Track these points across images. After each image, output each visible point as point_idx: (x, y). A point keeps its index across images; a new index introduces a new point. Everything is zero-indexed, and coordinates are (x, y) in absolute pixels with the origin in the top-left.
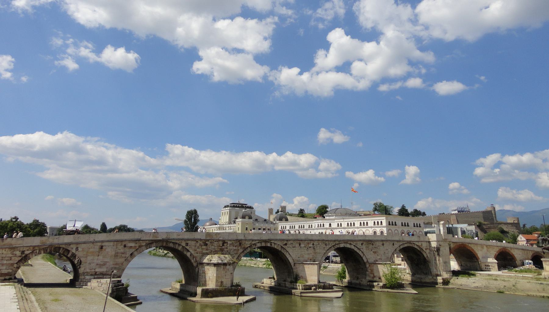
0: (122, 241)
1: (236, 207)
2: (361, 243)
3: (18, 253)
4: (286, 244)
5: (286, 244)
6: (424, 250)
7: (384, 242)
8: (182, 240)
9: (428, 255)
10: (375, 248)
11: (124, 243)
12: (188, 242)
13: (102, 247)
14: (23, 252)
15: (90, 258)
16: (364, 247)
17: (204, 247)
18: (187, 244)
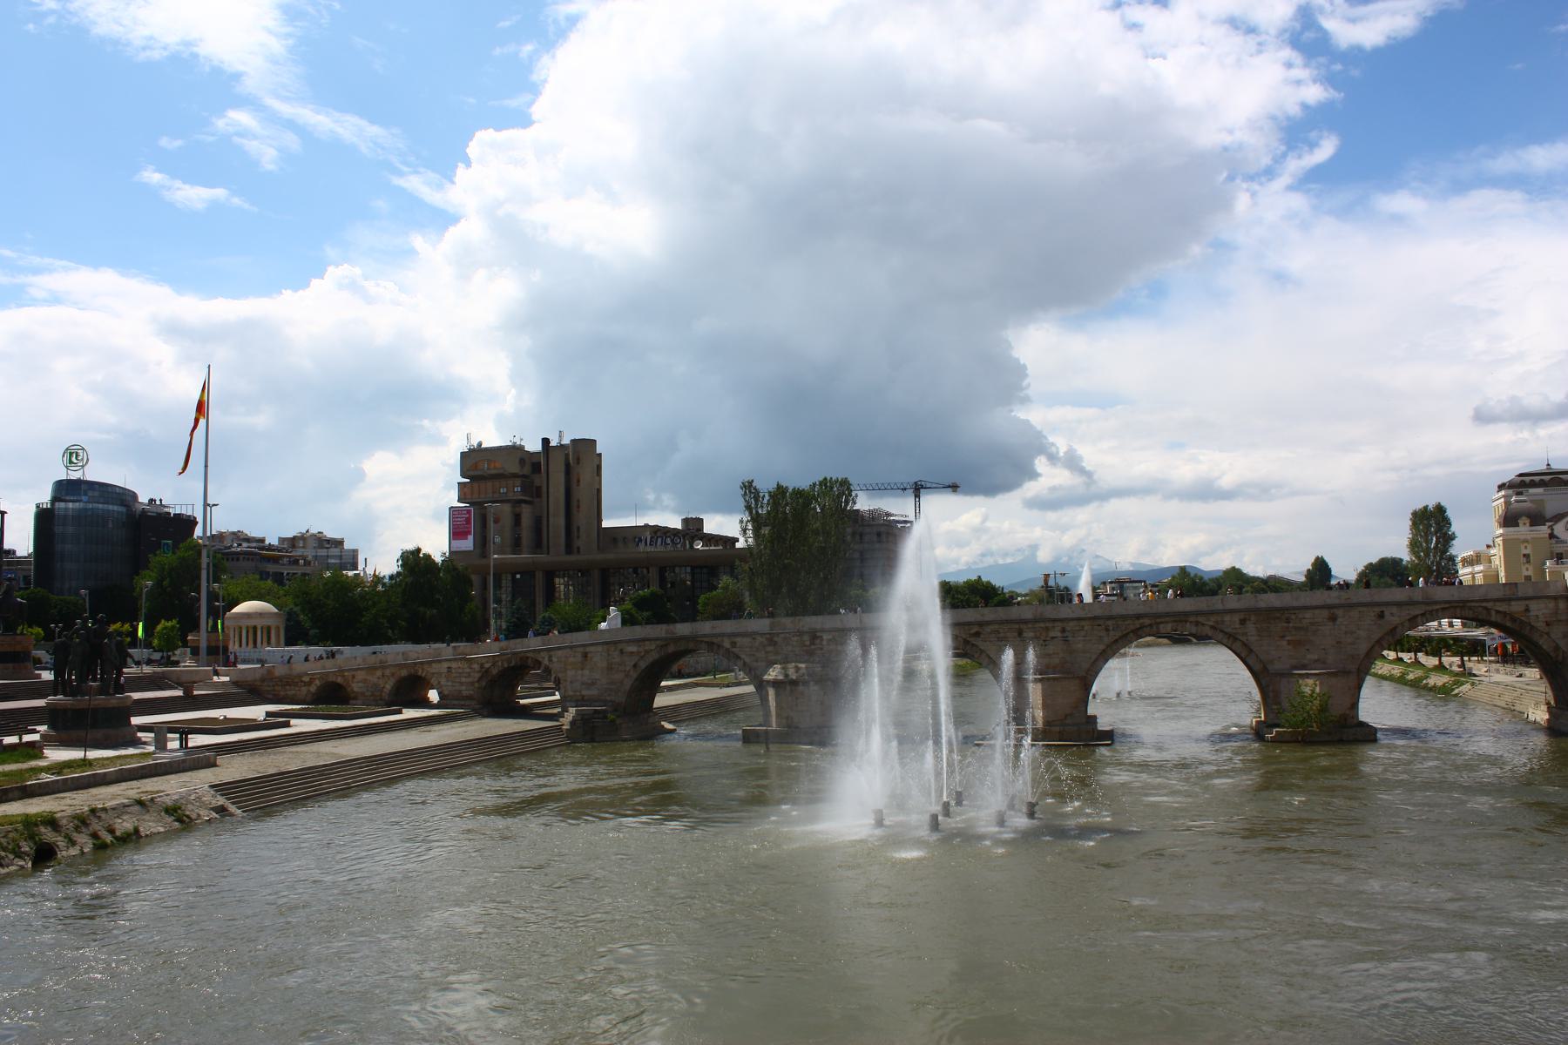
0: (615, 643)
1: (1533, 484)
2: (1236, 618)
3: (476, 666)
4: (977, 634)
5: (977, 634)
6: (1540, 625)
7: (1339, 612)
8: (723, 635)
9: (1562, 643)
10: (1296, 628)
11: (620, 646)
12: (738, 640)
13: (585, 655)
14: (482, 666)
15: (570, 673)
16: (1251, 628)
17: (770, 649)
18: (734, 644)
